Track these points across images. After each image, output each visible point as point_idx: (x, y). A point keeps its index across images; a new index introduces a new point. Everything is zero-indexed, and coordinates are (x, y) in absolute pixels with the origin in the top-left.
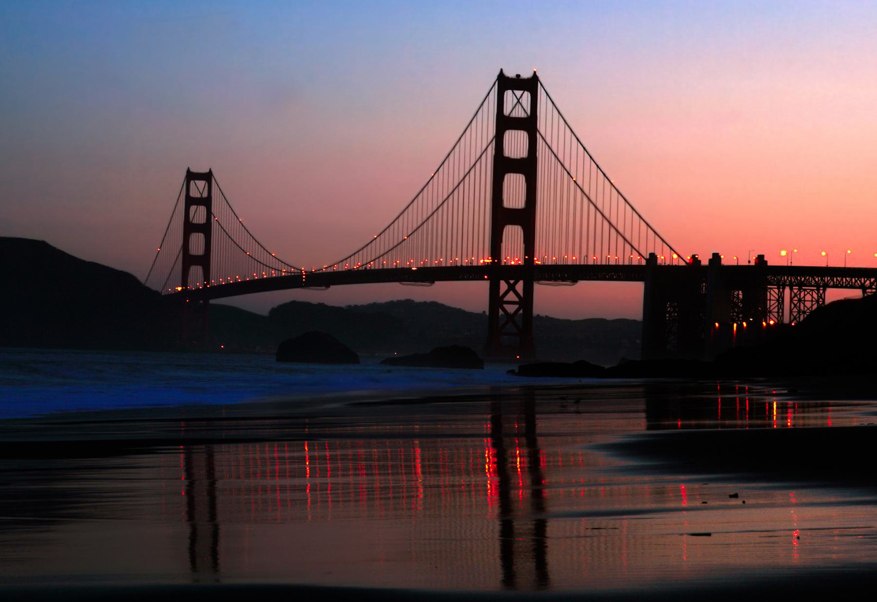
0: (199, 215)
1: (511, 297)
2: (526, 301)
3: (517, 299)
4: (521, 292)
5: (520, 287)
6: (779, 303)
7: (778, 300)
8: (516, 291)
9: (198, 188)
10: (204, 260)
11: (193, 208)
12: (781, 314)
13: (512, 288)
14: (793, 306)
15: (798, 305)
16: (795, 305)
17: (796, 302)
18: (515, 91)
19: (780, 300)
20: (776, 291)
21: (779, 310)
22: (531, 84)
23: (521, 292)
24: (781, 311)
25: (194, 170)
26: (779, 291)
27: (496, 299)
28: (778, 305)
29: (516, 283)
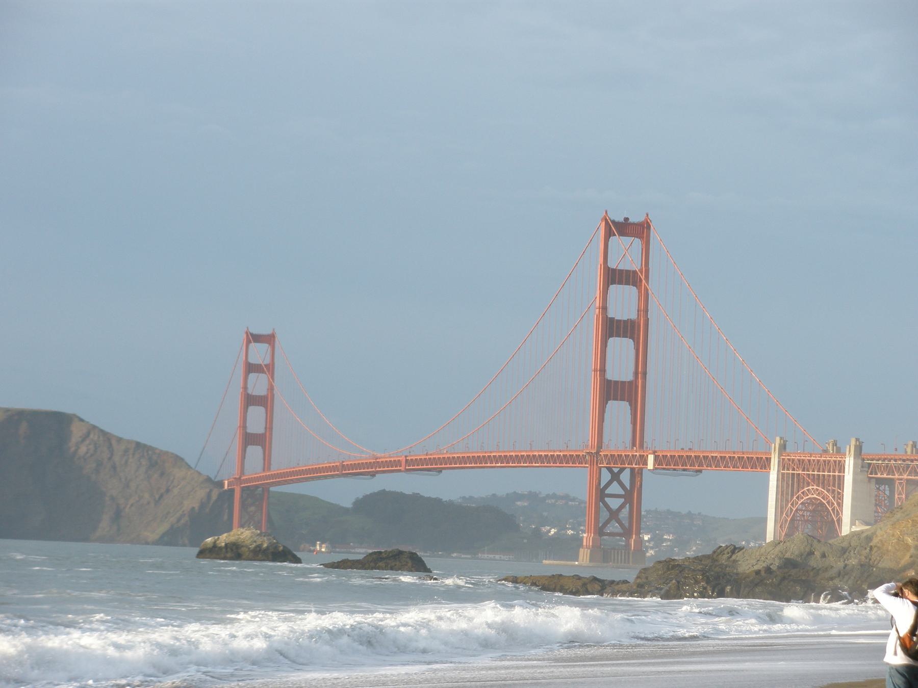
0: (258, 385)
1: (615, 488)
3: (622, 492)
4: (627, 485)
5: (625, 477)
8: (620, 480)
9: (259, 354)
11: (252, 376)
13: (615, 477)
18: (621, 237)
23: (627, 485)
25: (256, 331)
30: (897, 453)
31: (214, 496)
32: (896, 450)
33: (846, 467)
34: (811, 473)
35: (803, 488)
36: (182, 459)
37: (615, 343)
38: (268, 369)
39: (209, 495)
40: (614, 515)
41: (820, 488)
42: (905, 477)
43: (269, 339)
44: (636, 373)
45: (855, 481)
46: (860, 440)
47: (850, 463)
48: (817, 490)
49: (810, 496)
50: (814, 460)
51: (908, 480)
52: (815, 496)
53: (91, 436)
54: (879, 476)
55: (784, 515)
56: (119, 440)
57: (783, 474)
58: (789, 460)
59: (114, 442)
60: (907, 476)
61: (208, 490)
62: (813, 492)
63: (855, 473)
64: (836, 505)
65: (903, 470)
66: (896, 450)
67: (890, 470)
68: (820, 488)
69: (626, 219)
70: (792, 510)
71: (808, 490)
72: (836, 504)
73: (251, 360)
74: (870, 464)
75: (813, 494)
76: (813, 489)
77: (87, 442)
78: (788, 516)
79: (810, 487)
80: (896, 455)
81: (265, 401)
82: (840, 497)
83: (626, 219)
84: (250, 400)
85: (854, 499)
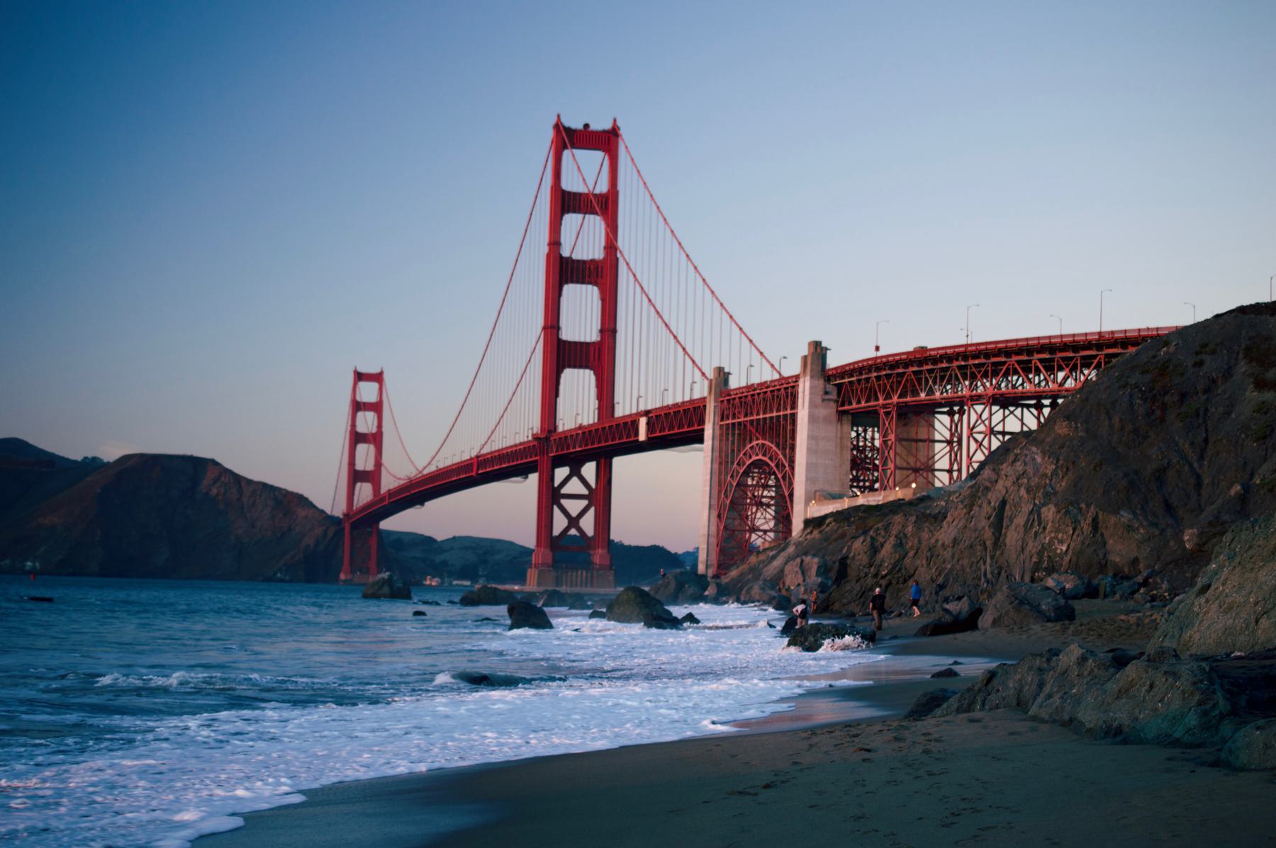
0: (366, 422)
2: (600, 497)
3: (585, 491)
4: (592, 480)
5: (589, 470)
6: (952, 449)
7: (949, 442)
9: (368, 392)
10: (373, 477)
12: (955, 474)
14: (973, 446)
15: (986, 443)
16: (980, 444)
17: (979, 437)
19: (954, 442)
20: (946, 419)
21: (951, 464)
22: (607, 141)
24: (955, 467)
25: (362, 370)
26: (952, 421)
27: (550, 497)
28: (950, 452)
29: (582, 463)
30: (880, 354)
31: (330, 534)
32: (877, 348)
33: (800, 395)
34: (755, 417)
35: (745, 446)
36: (306, 499)
37: (570, 290)
38: (377, 407)
39: (325, 534)
40: (573, 521)
41: (767, 443)
42: (895, 399)
43: (378, 378)
44: (602, 331)
45: (812, 419)
46: (823, 345)
47: (805, 389)
48: (763, 445)
49: (754, 458)
50: (759, 394)
51: (899, 407)
52: (760, 457)
53: (223, 479)
54: (854, 405)
55: (723, 496)
56: (250, 482)
57: (721, 425)
58: (729, 401)
59: (243, 484)
60: (899, 397)
61: (325, 528)
62: (756, 448)
63: (812, 405)
64: (787, 468)
65: (892, 387)
66: (877, 348)
67: (870, 391)
68: (767, 443)
69: (586, 126)
70: (731, 485)
71: (751, 448)
72: (787, 465)
73: (358, 399)
74: (839, 387)
75: (757, 455)
76: (757, 444)
77: (218, 484)
78: (727, 497)
79: (754, 443)
80: (876, 358)
81: (376, 439)
82: (793, 448)
83: (586, 126)
84: (357, 438)
85: (810, 451)
